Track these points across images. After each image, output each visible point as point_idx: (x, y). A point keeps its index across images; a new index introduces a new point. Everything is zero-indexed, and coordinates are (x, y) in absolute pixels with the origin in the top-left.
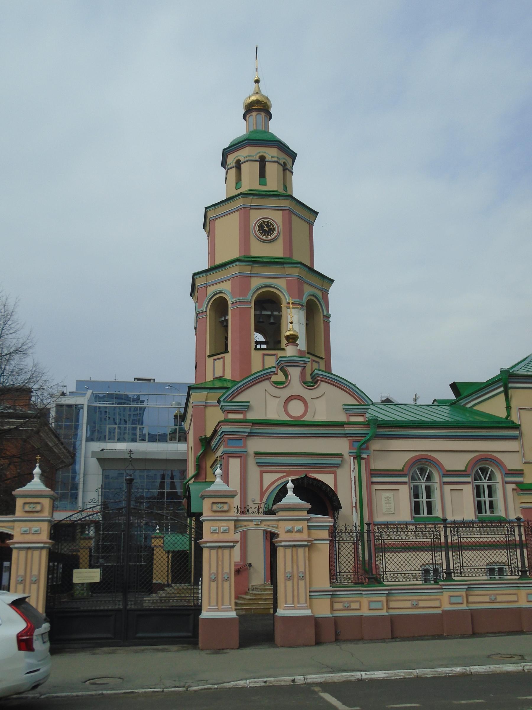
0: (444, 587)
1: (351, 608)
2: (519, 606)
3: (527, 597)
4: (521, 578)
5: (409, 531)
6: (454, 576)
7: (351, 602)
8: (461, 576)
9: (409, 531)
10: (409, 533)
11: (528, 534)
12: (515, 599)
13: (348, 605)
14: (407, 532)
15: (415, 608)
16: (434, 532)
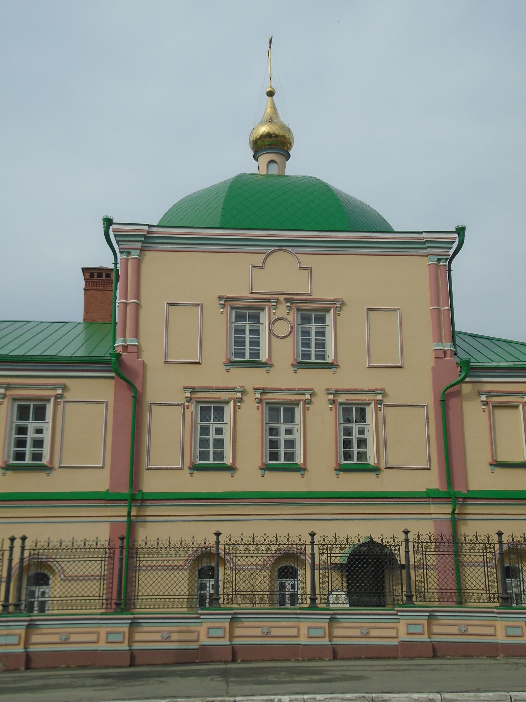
0: (202, 617)
1: (271, 634)
2: (496, 641)
3: (506, 631)
4: (502, 606)
5: (468, 543)
6: (416, 601)
7: (272, 628)
8: (425, 601)
9: (468, 543)
10: (468, 545)
11: (418, 550)
12: (520, 634)
13: (367, 632)
14: (465, 543)
15: (365, 637)
16: (487, 545)
